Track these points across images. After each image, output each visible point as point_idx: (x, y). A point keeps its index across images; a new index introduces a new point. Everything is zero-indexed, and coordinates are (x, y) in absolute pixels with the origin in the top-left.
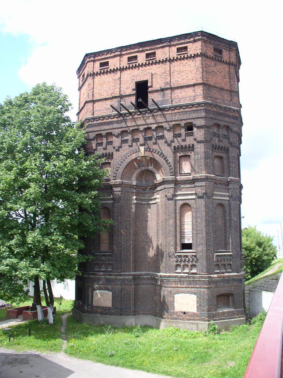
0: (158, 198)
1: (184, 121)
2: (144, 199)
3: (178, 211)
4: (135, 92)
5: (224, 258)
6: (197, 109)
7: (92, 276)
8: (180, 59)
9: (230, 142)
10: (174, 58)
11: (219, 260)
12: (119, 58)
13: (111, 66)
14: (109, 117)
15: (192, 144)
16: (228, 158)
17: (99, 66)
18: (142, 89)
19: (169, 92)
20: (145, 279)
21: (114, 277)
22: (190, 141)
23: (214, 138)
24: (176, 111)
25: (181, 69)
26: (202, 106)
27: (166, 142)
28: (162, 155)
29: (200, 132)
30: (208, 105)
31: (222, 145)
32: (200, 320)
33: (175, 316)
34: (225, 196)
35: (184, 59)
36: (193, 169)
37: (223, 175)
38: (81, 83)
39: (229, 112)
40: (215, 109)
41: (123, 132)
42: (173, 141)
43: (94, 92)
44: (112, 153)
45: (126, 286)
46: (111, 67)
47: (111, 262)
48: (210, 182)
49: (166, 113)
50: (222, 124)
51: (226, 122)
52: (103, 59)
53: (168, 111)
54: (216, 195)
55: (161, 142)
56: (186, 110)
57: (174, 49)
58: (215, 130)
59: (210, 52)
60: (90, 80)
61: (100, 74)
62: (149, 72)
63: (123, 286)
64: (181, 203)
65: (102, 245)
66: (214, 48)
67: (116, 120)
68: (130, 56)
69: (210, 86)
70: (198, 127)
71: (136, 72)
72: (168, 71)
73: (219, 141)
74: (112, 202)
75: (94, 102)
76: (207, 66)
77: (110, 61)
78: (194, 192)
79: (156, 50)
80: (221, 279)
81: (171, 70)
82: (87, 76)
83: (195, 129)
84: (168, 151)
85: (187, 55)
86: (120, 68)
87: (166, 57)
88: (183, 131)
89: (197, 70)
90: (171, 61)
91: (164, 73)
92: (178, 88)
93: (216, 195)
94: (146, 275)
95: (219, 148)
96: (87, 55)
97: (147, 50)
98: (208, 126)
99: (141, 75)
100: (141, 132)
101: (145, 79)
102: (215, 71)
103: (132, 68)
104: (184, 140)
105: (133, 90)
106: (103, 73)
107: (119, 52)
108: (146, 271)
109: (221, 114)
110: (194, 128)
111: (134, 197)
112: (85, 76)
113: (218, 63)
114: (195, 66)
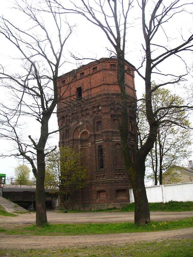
18: (79, 91)
42: (93, 115)
55: (88, 116)
78: (102, 139)
99: (78, 84)
101: (80, 86)
104: (97, 114)
105: (76, 92)
111: (80, 146)
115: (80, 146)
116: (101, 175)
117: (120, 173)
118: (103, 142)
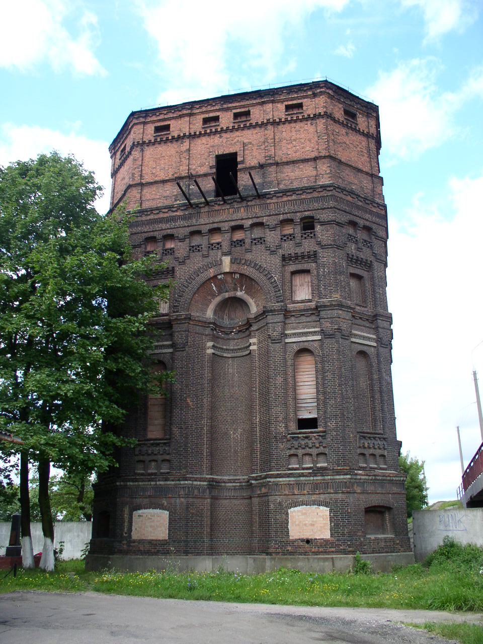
0: (254, 344)
1: (298, 214)
2: (227, 350)
3: (289, 362)
4: (214, 170)
5: (374, 444)
6: (321, 194)
7: (131, 483)
8: (290, 122)
9: (374, 253)
10: (280, 119)
11: (366, 445)
12: (187, 119)
13: (173, 131)
14: (170, 208)
15: (314, 252)
16: (372, 278)
17: (153, 132)
19: (273, 169)
20: (229, 489)
21: (173, 483)
22: (308, 246)
23: (349, 244)
24: (285, 199)
25: (293, 136)
26: (329, 191)
27: (268, 248)
28: (259, 268)
29: (327, 231)
30: (340, 191)
31: (362, 257)
32: (337, 552)
33: (289, 548)
34: (369, 339)
35: (295, 121)
36: (316, 290)
37: (365, 305)
38: (118, 162)
39: (370, 205)
40: (349, 198)
41: (193, 233)
42: (279, 247)
43: (144, 172)
44: (173, 268)
45: (195, 500)
46: (174, 132)
47: (167, 457)
48: (346, 312)
49: (268, 201)
50: (361, 223)
51: (367, 220)
52: (159, 121)
53: (271, 198)
54: (356, 336)
56: (303, 197)
57: (281, 107)
58: (351, 231)
59: (339, 114)
60: (136, 153)
61: (154, 144)
62: (238, 141)
63: (191, 500)
64: (296, 348)
65: (150, 428)
66: (344, 109)
67: (182, 214)
68: (207, 116)
69: (340, 162)
70: (323, 224)
71: (216, 141)
72: (272, 139)
73: (358, 249)
74: (171, 350)
75: (142, 185)
76: (335, 133)
77: (172, 123)
79: (250, 108)
80: (370, 478)
81: (276, 137)
82: (132, 149)
83: (318, 228)
84: (272, 263)
85: (302, 115)
86: (190, 134)
87: (268, 118)
88: (298, 230)
89: (318, 137)
90: (275, 123)
91: (264, 142)
92: (288, 163)
93: (356, 336)
94: (231, 482)
95: (357, 260)
96: (133, 114)
97: (235, 108)
98: (340, 223)
99: (224, 145)
100: (226, 232)
102: (348, 143)
103: (209, 135)
104: (299, 245)
105: (211, 167)
106: (160, 143)
107: (189, 109)
108: (229, 475)
109: (358, 207)
110: (316, 224)
111: (210, 344)
112: (128, 149)
113: (351, 131)
114: (316, 131)
115: (210, 344)
116: (308, 450)
117: (372, 451)
118: (319, 337)
